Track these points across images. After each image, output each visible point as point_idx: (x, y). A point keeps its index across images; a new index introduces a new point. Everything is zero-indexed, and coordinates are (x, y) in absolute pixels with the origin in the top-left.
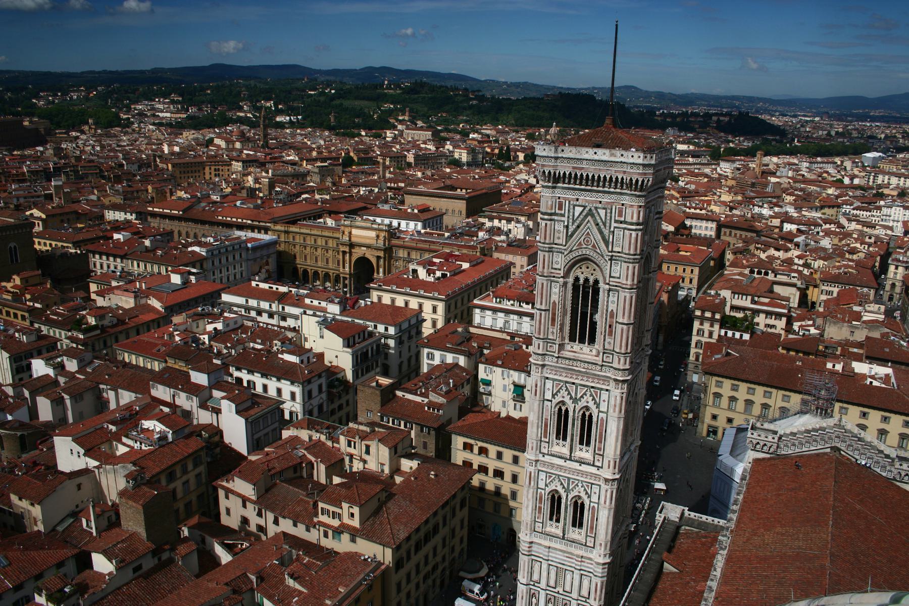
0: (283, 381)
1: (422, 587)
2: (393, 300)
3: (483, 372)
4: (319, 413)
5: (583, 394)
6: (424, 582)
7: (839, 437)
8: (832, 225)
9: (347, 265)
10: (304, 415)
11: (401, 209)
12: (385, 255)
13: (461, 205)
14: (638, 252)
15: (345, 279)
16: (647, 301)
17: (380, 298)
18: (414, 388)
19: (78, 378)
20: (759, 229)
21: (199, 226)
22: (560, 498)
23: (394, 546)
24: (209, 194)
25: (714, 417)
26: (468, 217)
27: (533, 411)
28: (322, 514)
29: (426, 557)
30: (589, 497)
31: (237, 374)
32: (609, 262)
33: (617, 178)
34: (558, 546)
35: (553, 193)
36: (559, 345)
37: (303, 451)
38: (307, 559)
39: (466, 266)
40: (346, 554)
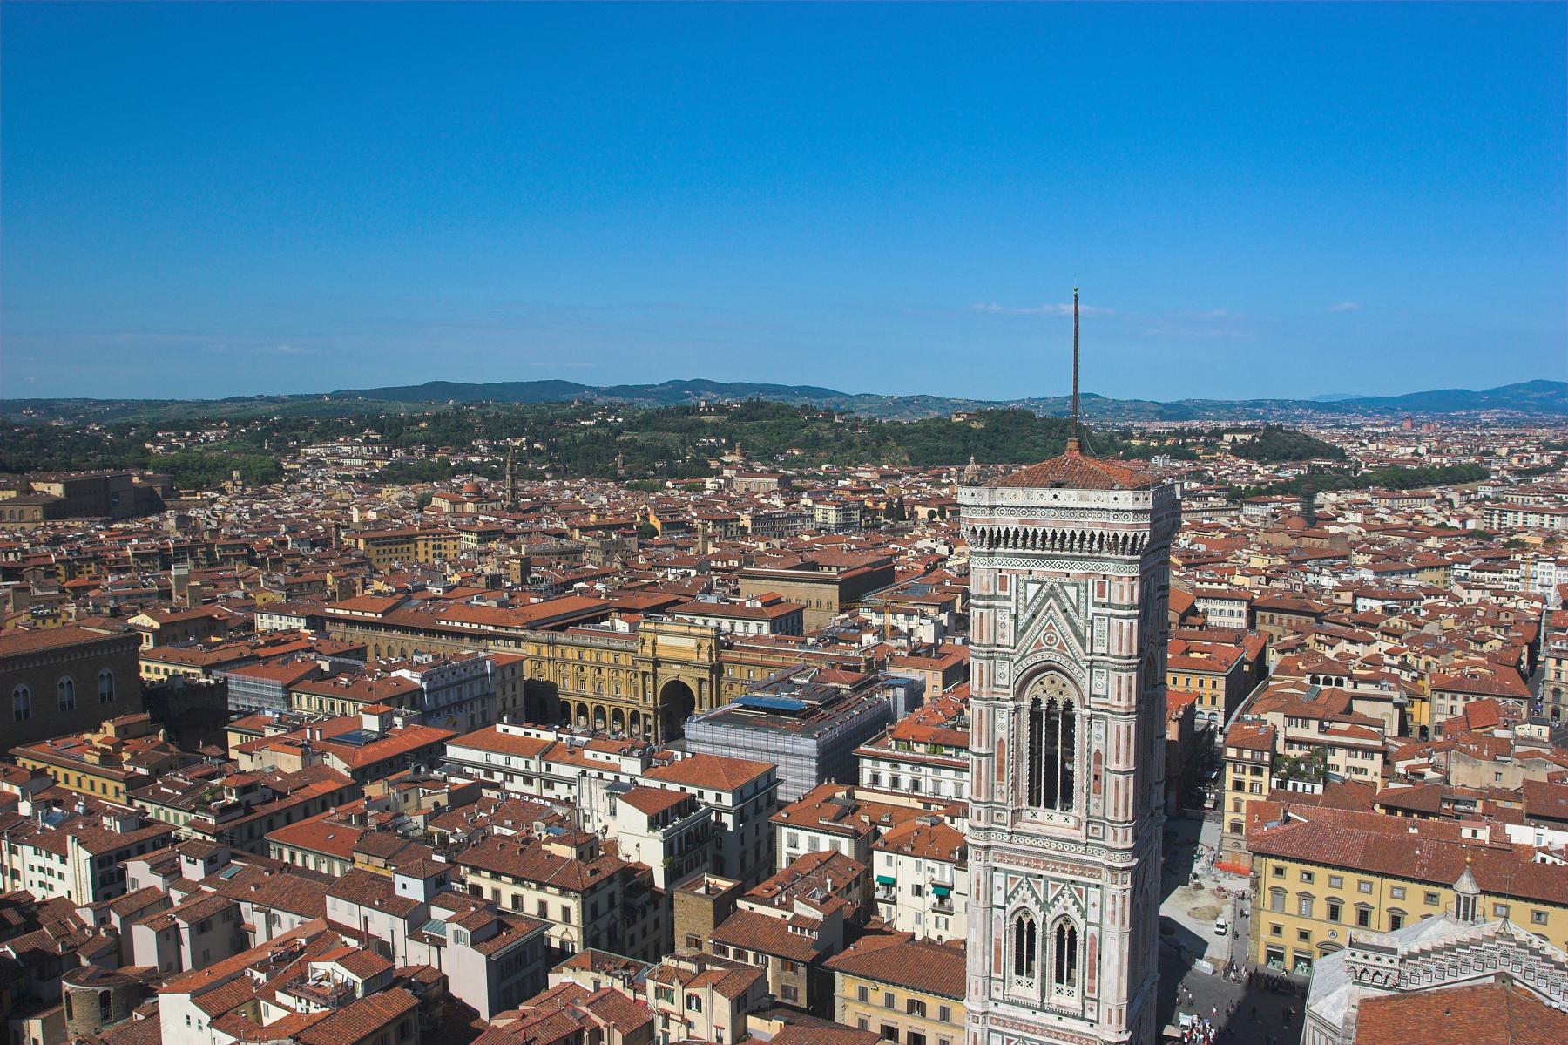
3: (881, 864)
5: (1058, 895)
7: (1508, 956)
9: (650, 695)
11: (734, 602)
12: (711, 677)
13: (831, 593)
14: (1135, 652)
15: (646, 716)
18: (768, 896)
19: (204, 892)
21: (409, 636)
24: (425, 585)
25: (1277, 930)
26: (842, 611)
31: (472, 879)
32: (1088, 671)
33: (1092, 535)
36: (1013, 812)
37: (584, 1009)
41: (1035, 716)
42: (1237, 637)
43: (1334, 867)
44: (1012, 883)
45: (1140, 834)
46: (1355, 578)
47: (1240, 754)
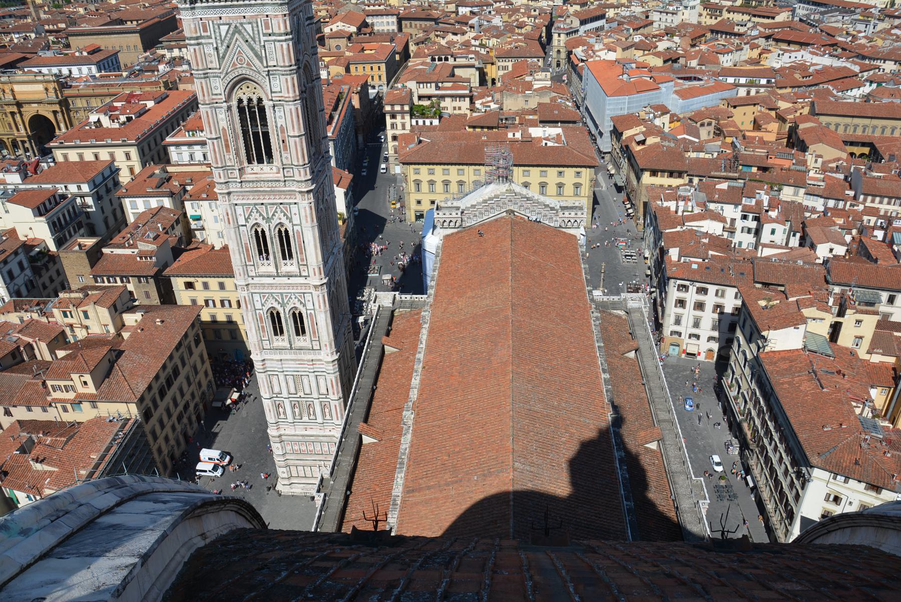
1: (179, 428)
2: (81, 156)
3: (190, 209)
4: (28, 291)
6: (179, 423)
7: (511, 201)
8: (502, 3)
10: (11, 296)
11: (67, 54)
13: (136, 39)
14: (293, 63)
16: (315, 109)
17: (65, 156)
18: (123, 242)
20: (436, 17)
22: (278, 313)
23: (136, 401)
25: (419, 202)
26: (145, 51)
27: (231, 239)
28: (55, 391)
29: (174, 400)
30: (304, 305)
32: (267, 78)
34: (288, 357)
35: (193, 14)
36: (239, 170)
37: (17, 335)
38: (50, 439)
40: (89, 421)
41: (241, 110)
43: (444, 164)
44: (247, 211)
45: (316, 170)
47: (393, 108)
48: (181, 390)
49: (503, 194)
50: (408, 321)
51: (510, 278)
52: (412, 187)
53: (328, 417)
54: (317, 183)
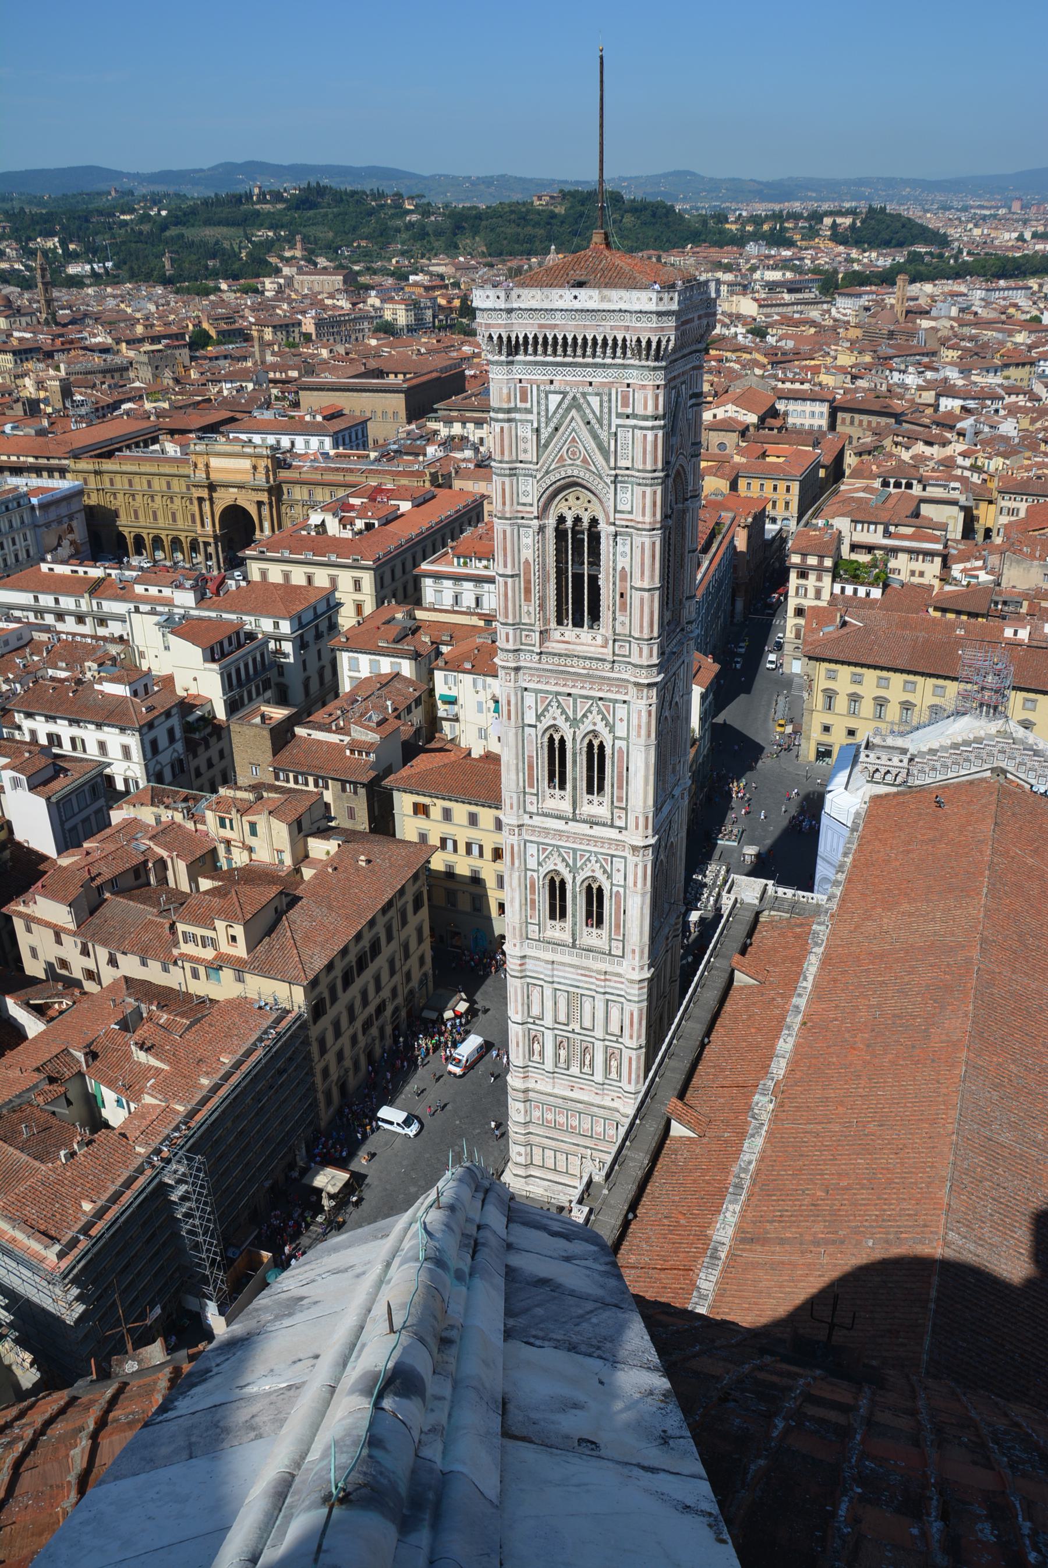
0: (105, 729)
1: (362, 1041)
2: (287, 576)
4: (174, 775)
8: (1021, 397)
9: (208, 521)
10: (149, 781)
11: (293, 417)
12: (270, 499)
13: (398, 402)
14: (660, 466)
15: (206, 544)
16: (683, 547)
17: (264, 573)
18: (328, 721)
22: (563, 883)
23: (306, 983)
25: (827, 729)
26: (409, 422)
27: (507, 745)
28: (186, 942)
29: (364, 994)
32: (612, 486)
33: (615, 339)
34: (567, 959)
35: (509, 372)
36: (541, 632)
38: (165, 1016)
39: (405, 506)
40: (229, 1001)
41: (560, 534)
42: (815, 438)
43: (882, 668)
44: (542, 702)
45: (668, 650)
46: (939, 376)
47: (804, 560)
48: (377, 979)
49: (990, 737)
50: (782, 935)
51: (985, 890)
52: (819, 700)
53: (614, 1075)
54: (666, 672)
